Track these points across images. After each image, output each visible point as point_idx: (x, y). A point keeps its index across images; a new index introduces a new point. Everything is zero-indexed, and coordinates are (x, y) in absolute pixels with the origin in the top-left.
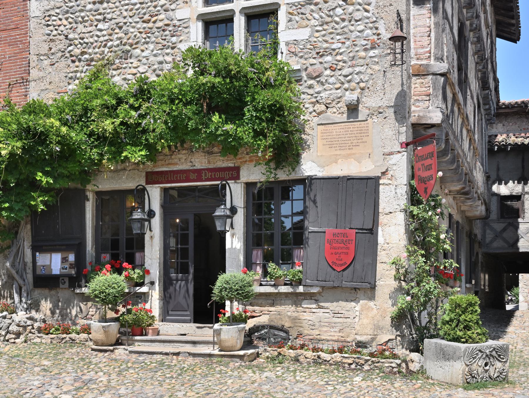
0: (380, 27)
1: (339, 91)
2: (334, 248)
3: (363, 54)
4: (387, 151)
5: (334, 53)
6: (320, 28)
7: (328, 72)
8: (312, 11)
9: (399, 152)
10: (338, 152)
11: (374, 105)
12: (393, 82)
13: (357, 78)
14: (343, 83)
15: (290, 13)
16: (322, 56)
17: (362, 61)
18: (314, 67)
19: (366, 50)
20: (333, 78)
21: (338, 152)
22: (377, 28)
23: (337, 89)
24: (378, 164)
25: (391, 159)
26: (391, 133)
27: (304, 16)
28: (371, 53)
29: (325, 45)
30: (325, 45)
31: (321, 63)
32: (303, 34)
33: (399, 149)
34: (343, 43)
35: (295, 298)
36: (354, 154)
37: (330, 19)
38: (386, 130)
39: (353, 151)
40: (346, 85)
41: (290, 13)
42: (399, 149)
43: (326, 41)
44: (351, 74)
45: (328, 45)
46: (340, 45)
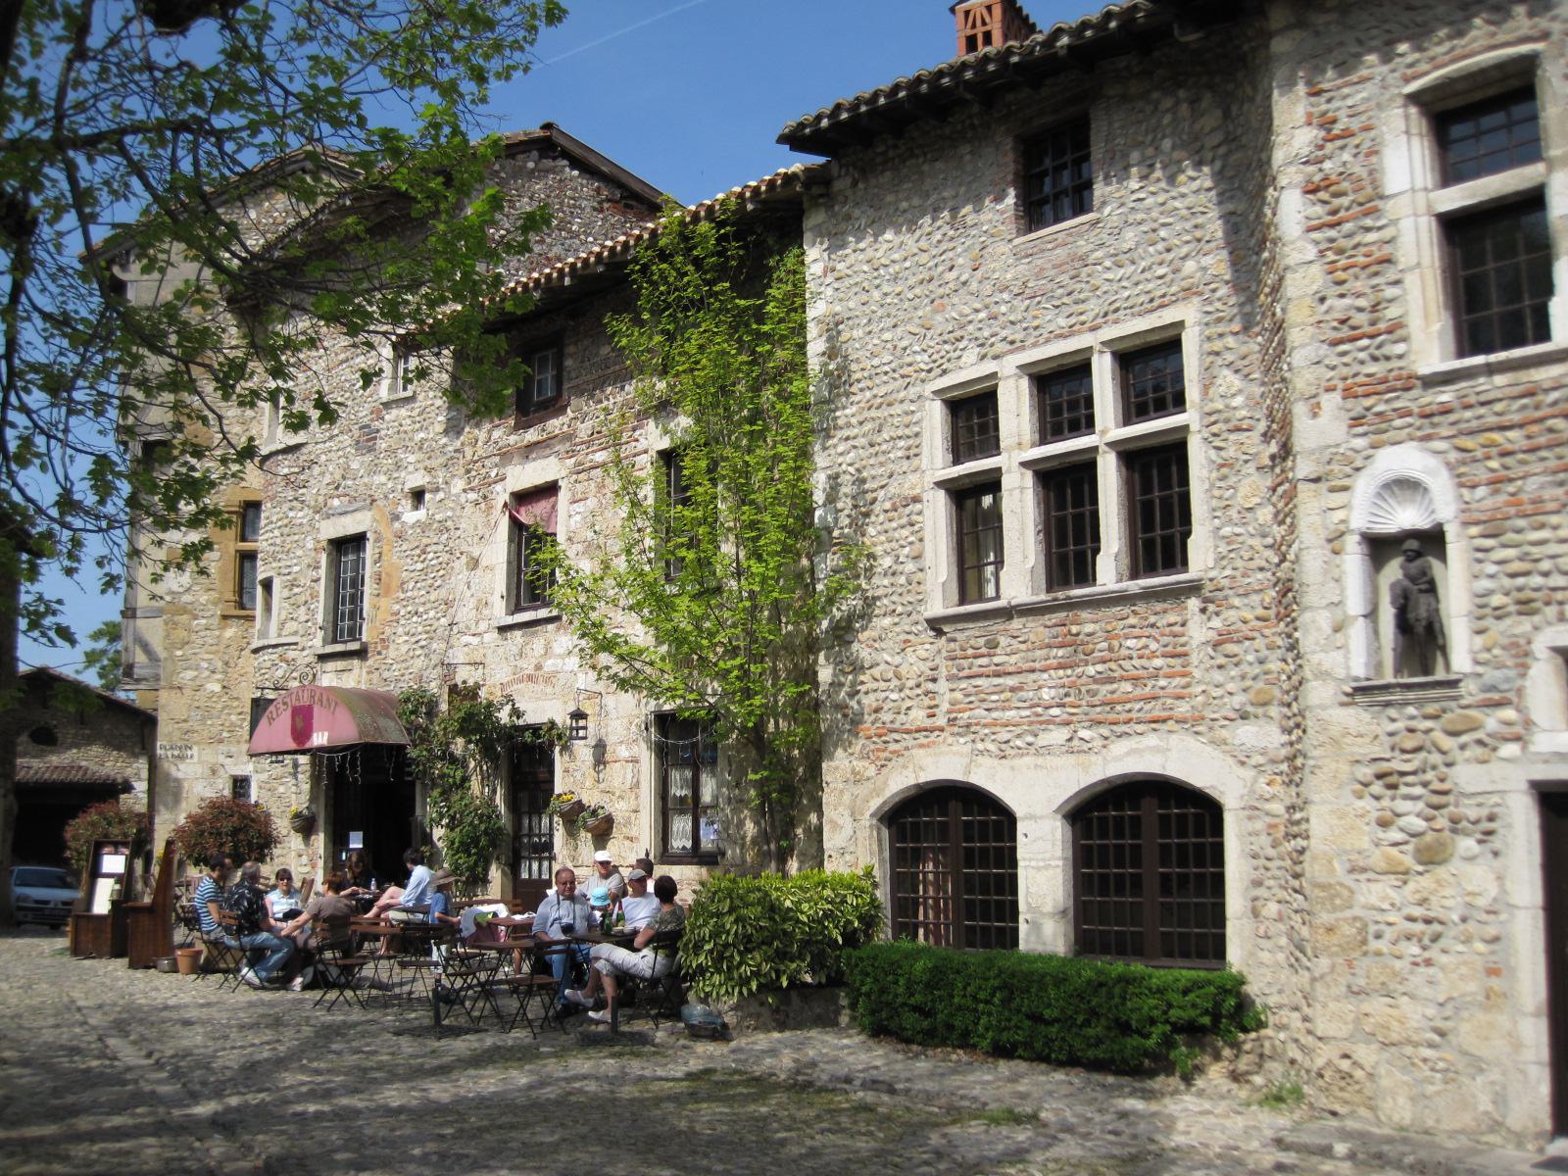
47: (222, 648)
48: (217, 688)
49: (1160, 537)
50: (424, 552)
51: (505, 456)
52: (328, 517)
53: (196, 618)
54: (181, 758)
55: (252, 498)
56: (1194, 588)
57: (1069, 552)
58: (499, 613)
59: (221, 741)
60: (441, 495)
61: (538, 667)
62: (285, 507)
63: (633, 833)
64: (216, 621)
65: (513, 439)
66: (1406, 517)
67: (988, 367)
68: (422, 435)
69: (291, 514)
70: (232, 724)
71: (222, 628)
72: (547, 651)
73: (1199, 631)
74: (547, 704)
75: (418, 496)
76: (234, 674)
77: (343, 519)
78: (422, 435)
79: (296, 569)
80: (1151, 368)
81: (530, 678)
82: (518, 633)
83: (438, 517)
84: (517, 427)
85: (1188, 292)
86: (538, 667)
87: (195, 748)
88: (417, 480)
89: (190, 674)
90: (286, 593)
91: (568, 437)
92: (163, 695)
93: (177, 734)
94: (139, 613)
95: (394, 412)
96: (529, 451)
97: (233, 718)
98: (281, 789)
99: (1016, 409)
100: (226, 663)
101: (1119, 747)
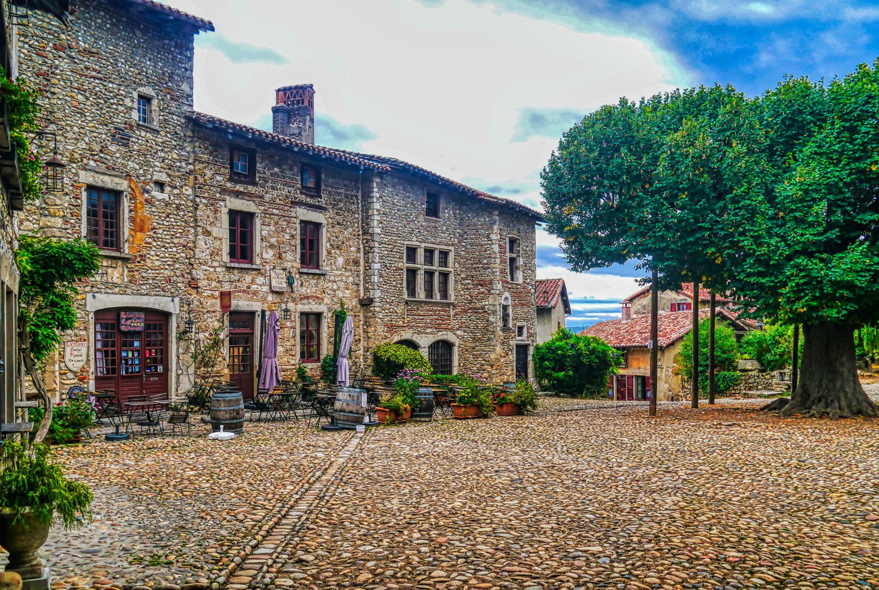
49: (445, 294)
50: (168, 216)
51: (224, 191)
52: (86, 170)
56: (453, 304)
57: (430, 292)
58: (226, 258)
60: (176, 191)
61: (249, 287)
63: (293, 353)
65: (229, 185)
66: (504, 303)
67: (419, 244)
68: (163, 154)
72: (253, 281)
73: (452, 313)
74: (254, 303)
75: (161, 185)
77: (101, 177)
78: (163, 154)
80: (444, 254)
81: (244, 291)
82: (236, 271)
83: (177, 202)
84: (230, 180)
85: (453, 245)
86: (249, 287)
88: (163, 177)
91: (262, 197)
95: (143, 133)
96: (237, 194)
99: (420, 255)
101: (440, 333)
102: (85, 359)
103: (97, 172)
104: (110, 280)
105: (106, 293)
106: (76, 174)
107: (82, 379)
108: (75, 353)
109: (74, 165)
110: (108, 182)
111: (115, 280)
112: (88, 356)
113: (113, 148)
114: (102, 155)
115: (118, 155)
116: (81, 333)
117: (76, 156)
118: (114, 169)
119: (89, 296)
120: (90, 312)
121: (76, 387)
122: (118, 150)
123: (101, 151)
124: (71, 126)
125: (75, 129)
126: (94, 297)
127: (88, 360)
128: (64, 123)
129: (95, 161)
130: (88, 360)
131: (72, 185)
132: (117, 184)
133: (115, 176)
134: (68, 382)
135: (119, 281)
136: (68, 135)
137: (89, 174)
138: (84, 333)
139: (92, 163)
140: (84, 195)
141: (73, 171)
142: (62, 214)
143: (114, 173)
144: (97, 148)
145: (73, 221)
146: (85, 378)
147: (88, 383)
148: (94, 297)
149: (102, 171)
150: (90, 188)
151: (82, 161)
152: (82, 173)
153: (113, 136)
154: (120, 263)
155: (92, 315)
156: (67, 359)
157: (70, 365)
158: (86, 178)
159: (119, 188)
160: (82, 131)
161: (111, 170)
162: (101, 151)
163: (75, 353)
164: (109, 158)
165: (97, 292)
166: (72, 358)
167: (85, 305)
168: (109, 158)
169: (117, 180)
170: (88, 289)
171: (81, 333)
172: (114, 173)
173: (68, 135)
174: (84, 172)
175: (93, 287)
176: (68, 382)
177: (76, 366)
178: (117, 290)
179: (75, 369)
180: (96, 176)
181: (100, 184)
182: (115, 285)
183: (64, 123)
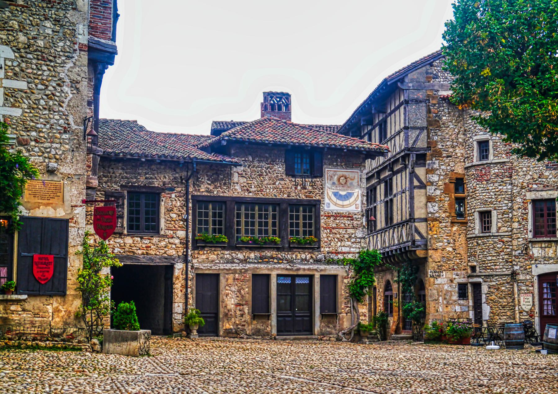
0: (70, 119)
1: (41, 158)
2: (40, 268)
3: (58, 135)
4: (74, 203)
5: (38, 130)
6: (28, 111)
7: (33, 143)
8: (22, 96)
9: (81, 206)
10: (40, 201)
11: (65, 172)
12: (78, 159)
13: (53, 152)
14: (43, 153)
15: (6, 94)
16: (28, 131)
17: (58, 141)
18: (23, 137)
19: (60, 133)
20: (37, 148)
21: (40, 201)
22: (68, 120)
23: (39, 156)
24: (68, 212)
25: (75, 210)
26: (76, 192)
27: (17, 99)
28: (64, 136)
29: (32, 124)
30: (32, 124)
31: (29, 135)
32: (17, 113)
33: (81, 204)
34: (45, 125)
35: (5, 304)
36: (52, 204)
37: (35, 106)
38: (73, 190)
39: (50, 202)
40: (46, 155)
41: (6, 94)
42: (81, 204)
43: (32, 121)
44: (49, 147)
45: (34, 124)
46: (43, 126)
47: (452, 234)
48: (451, 249)
52: (530, 191)
53: (441, 222)
54: (439, 276)
55: (459, 177)
59: (454, 270)
62: (496, 185)
64: (449, 224)
69: (500, 187)
70: (458, 263)
71: (452, 227)
76: (457, 244)
77: (540, 193)
79: (504, 208)
87: (444, 273)
89: (441, 244)
90: (500, 216)
92: (430, 252)
93: (436, 267)
94: (416, 221)
97: (458, 261)
98: (503, 288)
100: (454, 240)
102: (532, 304)
103: (538, 191)
104: (547, 256)
105: (544, 263)
106: (525, 195)
107: (531, 316)
108: (526, 300)
109: (523, 190)
110: (545, 195)
111: (550, 255)
112: (533, 302)
113: (547, 174)
114: (540, 180)
115: (551, 176)
116: (530, 288)
117: (525, 184)
118: (548, 186)
119: (534, 266)
120: (534, 276)
121: (528, 321)
122: (550, 174)
123: (539, 177)
124: (522, 168)
125: (525, 169)
126: (537, 267)
127: (534, 305)
128: (517, 168)
129: (536, 184)
130: (534, 305)
131: (523, 202)
132: (551, 195)
133: (550, 190)
134: (523, 317)
135: (553, 256)
136: (520, 174)
137: (533, 193)
138: (532, 288)
139: (535, 186)
140: (530, 207)
141: (523, 194)
142: (517, 220)
143: (548, 188)
144: (536, 176)
145: (523, 223)
146: (533, 316)
147: (534, 319)
148: (537, 267)
149: (540, 189)
150: (534, 201)
151: (528, 186)
152: (528, 194)
153: (547, 166)
154: (553, 244)
155: (535, 278)
156: (522, 304)
157: (523, 307)
158: (530, 196)
159: (552, 197)
160: (528, 169)
161: (546, 187)
162: (539, 177)
163: (526, 300)
164: (544, 180)
165: (538, 264)
166: (524, 303)
167: (531, 272)
168: (544, 180)
169: (550, 192)
170: (533, 262)
171: (530, 288)
172: (548, 188)
173: (520, 174)
174: (529, 193)
175: (536, 260)
176: (523, 317)
177: (527, 308)
178: (551, 261)
179: (527, 310)
180: (537, 193)
181: (540, 197)
182: (551, 258)
183: (517, 168)
